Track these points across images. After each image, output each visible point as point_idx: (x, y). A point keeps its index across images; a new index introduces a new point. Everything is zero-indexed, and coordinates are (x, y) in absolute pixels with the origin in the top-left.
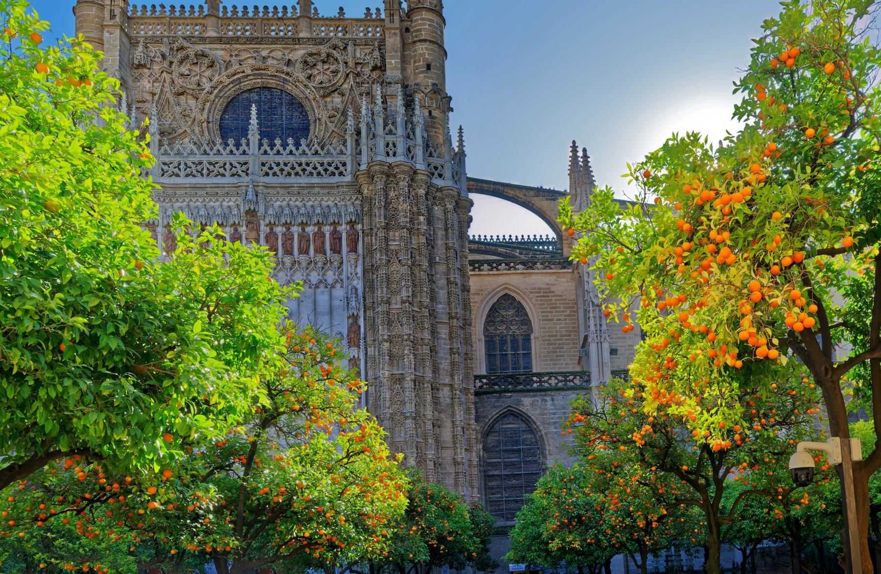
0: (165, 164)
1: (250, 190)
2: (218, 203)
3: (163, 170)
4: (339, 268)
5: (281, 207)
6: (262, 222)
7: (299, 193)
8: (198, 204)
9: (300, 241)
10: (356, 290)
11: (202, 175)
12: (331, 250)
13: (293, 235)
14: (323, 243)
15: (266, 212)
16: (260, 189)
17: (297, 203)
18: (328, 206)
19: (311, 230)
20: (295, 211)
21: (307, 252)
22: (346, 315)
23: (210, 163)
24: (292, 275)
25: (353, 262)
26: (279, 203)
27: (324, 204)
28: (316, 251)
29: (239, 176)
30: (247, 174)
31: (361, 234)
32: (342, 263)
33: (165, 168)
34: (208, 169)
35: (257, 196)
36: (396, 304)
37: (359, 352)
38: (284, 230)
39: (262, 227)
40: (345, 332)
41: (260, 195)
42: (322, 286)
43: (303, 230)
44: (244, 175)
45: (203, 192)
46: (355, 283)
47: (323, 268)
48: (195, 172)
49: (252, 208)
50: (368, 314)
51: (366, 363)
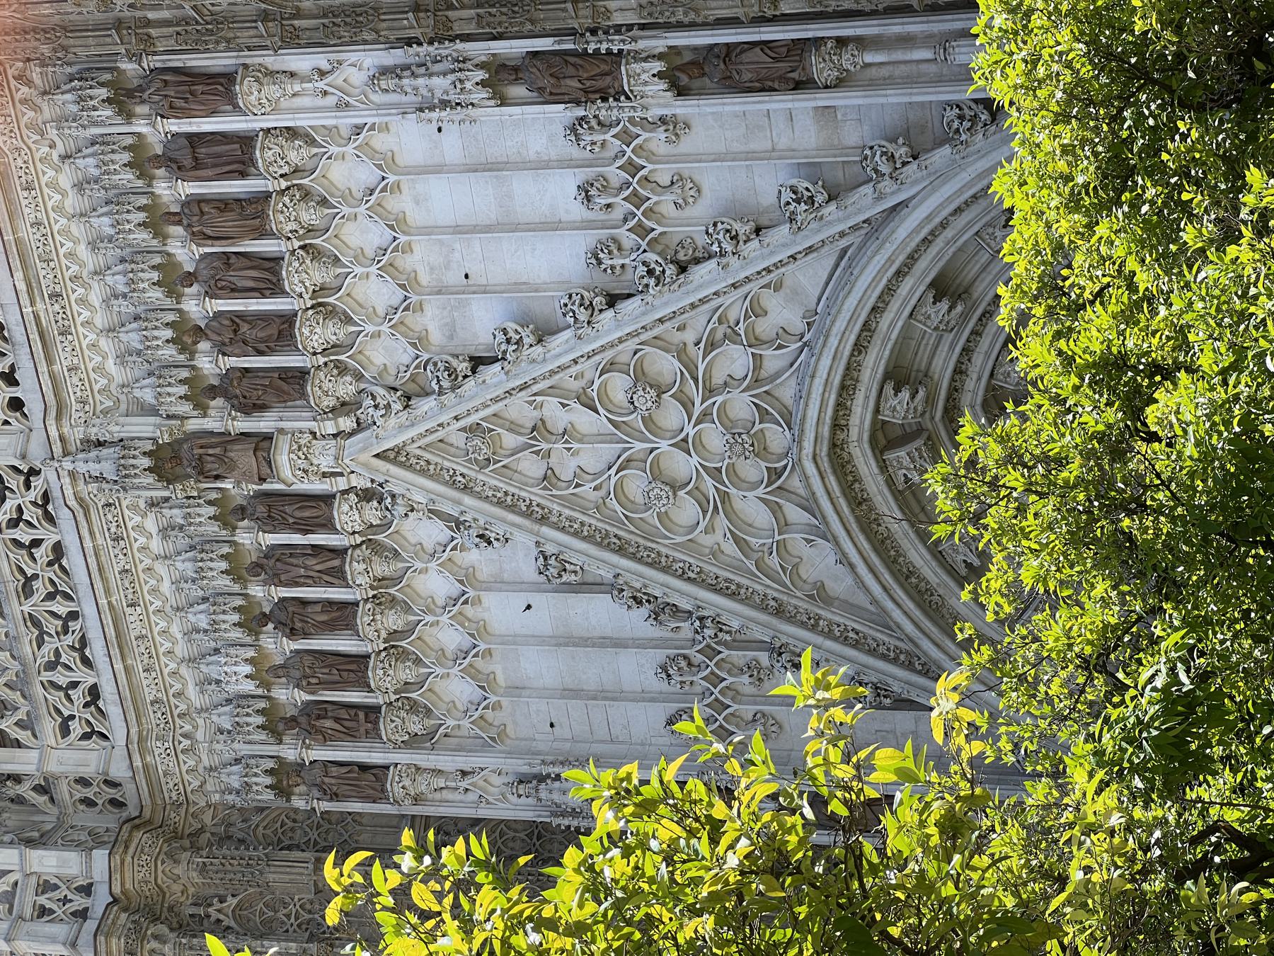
0: (65, 731)
1: (82, 468)
2: (161, 568)
3: (86, 736)
4: (311, 142)
5: (121, 359)
6: (194, 425)
7: (55, 296)
8: (175, 630)
9: (235, 291)
10: (385, 71)
11: (74, 615)
12: (243, 175)
13: (219, 315)
14: (224, 204)
15: (154, 412)
16: (76, 435)
17: (95, 298)
18: (79, 187)
19: (185, 252)
20: (125, 307)
21: (274, 262)
22: (491, 114)
23: (27, 589)
24: (371, 316)
25: (272, 91)
26: (110, 365)
27: (72, 202)
28: (263, 233)
29: (46, 497)
30: (33, 472)
31: (156, 61)
32: (292, 133)
33: (77, 728)
34: (50, 597)
35: (100, 444)
36: (292, 304)
37: (638, 57)
38: (204, 346)
39: (211, 424)
40: (560, 114)
41: (94, 433)
42: (394, 204)
43: (190, 278)
44: (37, 482)
45: (132, 616)
46: (358, 78)
47: (324, 202)
48: (69, 639)
49: (146, 462)
50: (471, 29)
51: (680, 26)
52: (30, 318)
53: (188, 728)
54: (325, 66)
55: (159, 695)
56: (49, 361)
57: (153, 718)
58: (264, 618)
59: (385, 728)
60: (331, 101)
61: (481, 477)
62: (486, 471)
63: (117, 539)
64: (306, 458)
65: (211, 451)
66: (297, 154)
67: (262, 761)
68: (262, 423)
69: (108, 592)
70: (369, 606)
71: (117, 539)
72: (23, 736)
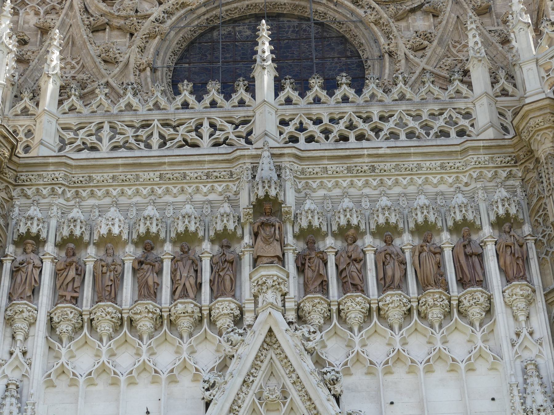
3: (62, 140)
52: (360, 152)
53: (69, 195)
54: (537, 336)
55: (95, 181)
56: (330, 158)
57: (79, 175)
58: (149, 249)
59: (66, 307)
60: (514, 337)
61: (251, 393)
62: (254, 397)
63: (208, 175)
64: (273, 286)
65: (277, 232)
66: (476, 313)
67: (46, 230)
68: (291, 267)
69: (172, 164)
70: (158, 311)
71: (208, 175)
72: (66, 105)
